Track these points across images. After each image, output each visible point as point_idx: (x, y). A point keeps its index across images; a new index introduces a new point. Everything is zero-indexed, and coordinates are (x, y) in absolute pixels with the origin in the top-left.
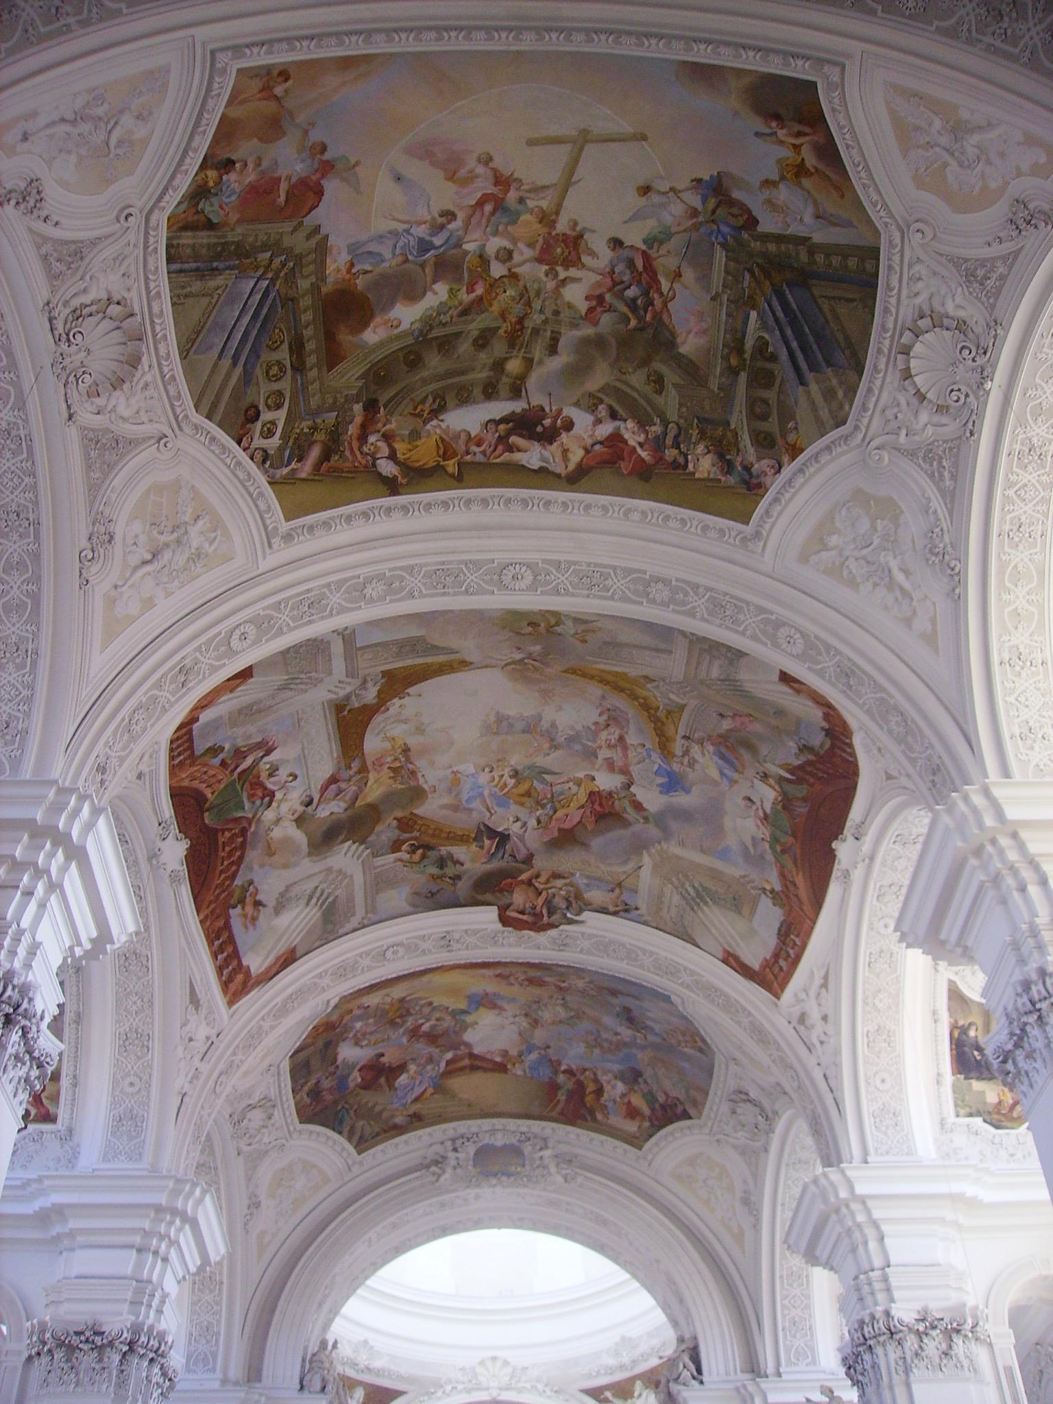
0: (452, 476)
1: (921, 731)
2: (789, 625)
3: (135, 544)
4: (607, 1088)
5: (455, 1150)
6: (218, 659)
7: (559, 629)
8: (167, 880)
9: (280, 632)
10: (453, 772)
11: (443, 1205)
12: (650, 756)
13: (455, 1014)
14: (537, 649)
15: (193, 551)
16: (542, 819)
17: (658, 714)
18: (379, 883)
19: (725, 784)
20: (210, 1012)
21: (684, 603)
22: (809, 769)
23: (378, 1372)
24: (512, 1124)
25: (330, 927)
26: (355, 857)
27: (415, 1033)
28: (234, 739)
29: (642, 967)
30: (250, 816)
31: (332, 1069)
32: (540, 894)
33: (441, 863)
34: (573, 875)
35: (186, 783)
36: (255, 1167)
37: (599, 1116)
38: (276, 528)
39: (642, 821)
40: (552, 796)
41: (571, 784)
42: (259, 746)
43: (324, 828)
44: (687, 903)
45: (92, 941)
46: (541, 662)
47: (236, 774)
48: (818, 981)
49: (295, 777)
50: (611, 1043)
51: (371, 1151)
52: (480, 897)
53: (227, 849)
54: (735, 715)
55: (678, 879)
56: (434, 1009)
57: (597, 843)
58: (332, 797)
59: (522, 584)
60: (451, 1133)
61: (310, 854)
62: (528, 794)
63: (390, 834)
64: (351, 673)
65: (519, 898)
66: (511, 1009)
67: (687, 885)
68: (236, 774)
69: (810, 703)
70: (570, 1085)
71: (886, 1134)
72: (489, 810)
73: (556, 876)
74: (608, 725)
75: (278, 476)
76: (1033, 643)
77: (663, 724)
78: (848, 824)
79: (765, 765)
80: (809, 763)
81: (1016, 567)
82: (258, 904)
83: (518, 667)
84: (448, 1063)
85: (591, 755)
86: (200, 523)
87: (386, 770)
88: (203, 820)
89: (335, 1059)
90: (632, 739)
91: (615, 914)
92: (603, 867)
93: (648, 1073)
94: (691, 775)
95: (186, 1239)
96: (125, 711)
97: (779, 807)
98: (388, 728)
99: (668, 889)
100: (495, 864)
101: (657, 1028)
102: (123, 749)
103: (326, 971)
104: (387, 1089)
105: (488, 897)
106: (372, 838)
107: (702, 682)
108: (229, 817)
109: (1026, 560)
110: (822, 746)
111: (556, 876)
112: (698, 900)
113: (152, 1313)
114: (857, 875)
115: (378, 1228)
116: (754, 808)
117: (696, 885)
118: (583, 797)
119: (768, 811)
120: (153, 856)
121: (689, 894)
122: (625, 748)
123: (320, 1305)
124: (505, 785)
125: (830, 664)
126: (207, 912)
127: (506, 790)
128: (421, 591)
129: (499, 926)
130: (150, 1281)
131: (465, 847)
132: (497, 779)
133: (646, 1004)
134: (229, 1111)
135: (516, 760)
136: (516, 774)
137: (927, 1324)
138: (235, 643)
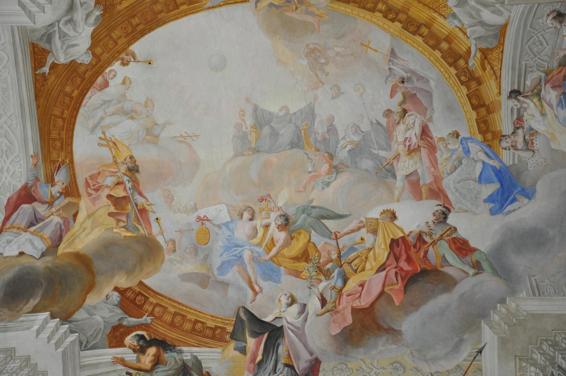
10: (199, 219)
12: (467, 152)
17: (471, 62)
26: (53, 341)
39: (471, 271)
40: (339, 257)
43: (9, 275)
55: (543, 354)
58: (23, 225)
62: (304, 256)
63: (107, 315)
74: (405, 111)
77: (479, 82)
87: (105, 201)
98: (107, 121)
106: (80, 315)
122: (432, 149)
124: (273, 242)
127: (274, 251)
131: (219, 350)
132: (261, 232)
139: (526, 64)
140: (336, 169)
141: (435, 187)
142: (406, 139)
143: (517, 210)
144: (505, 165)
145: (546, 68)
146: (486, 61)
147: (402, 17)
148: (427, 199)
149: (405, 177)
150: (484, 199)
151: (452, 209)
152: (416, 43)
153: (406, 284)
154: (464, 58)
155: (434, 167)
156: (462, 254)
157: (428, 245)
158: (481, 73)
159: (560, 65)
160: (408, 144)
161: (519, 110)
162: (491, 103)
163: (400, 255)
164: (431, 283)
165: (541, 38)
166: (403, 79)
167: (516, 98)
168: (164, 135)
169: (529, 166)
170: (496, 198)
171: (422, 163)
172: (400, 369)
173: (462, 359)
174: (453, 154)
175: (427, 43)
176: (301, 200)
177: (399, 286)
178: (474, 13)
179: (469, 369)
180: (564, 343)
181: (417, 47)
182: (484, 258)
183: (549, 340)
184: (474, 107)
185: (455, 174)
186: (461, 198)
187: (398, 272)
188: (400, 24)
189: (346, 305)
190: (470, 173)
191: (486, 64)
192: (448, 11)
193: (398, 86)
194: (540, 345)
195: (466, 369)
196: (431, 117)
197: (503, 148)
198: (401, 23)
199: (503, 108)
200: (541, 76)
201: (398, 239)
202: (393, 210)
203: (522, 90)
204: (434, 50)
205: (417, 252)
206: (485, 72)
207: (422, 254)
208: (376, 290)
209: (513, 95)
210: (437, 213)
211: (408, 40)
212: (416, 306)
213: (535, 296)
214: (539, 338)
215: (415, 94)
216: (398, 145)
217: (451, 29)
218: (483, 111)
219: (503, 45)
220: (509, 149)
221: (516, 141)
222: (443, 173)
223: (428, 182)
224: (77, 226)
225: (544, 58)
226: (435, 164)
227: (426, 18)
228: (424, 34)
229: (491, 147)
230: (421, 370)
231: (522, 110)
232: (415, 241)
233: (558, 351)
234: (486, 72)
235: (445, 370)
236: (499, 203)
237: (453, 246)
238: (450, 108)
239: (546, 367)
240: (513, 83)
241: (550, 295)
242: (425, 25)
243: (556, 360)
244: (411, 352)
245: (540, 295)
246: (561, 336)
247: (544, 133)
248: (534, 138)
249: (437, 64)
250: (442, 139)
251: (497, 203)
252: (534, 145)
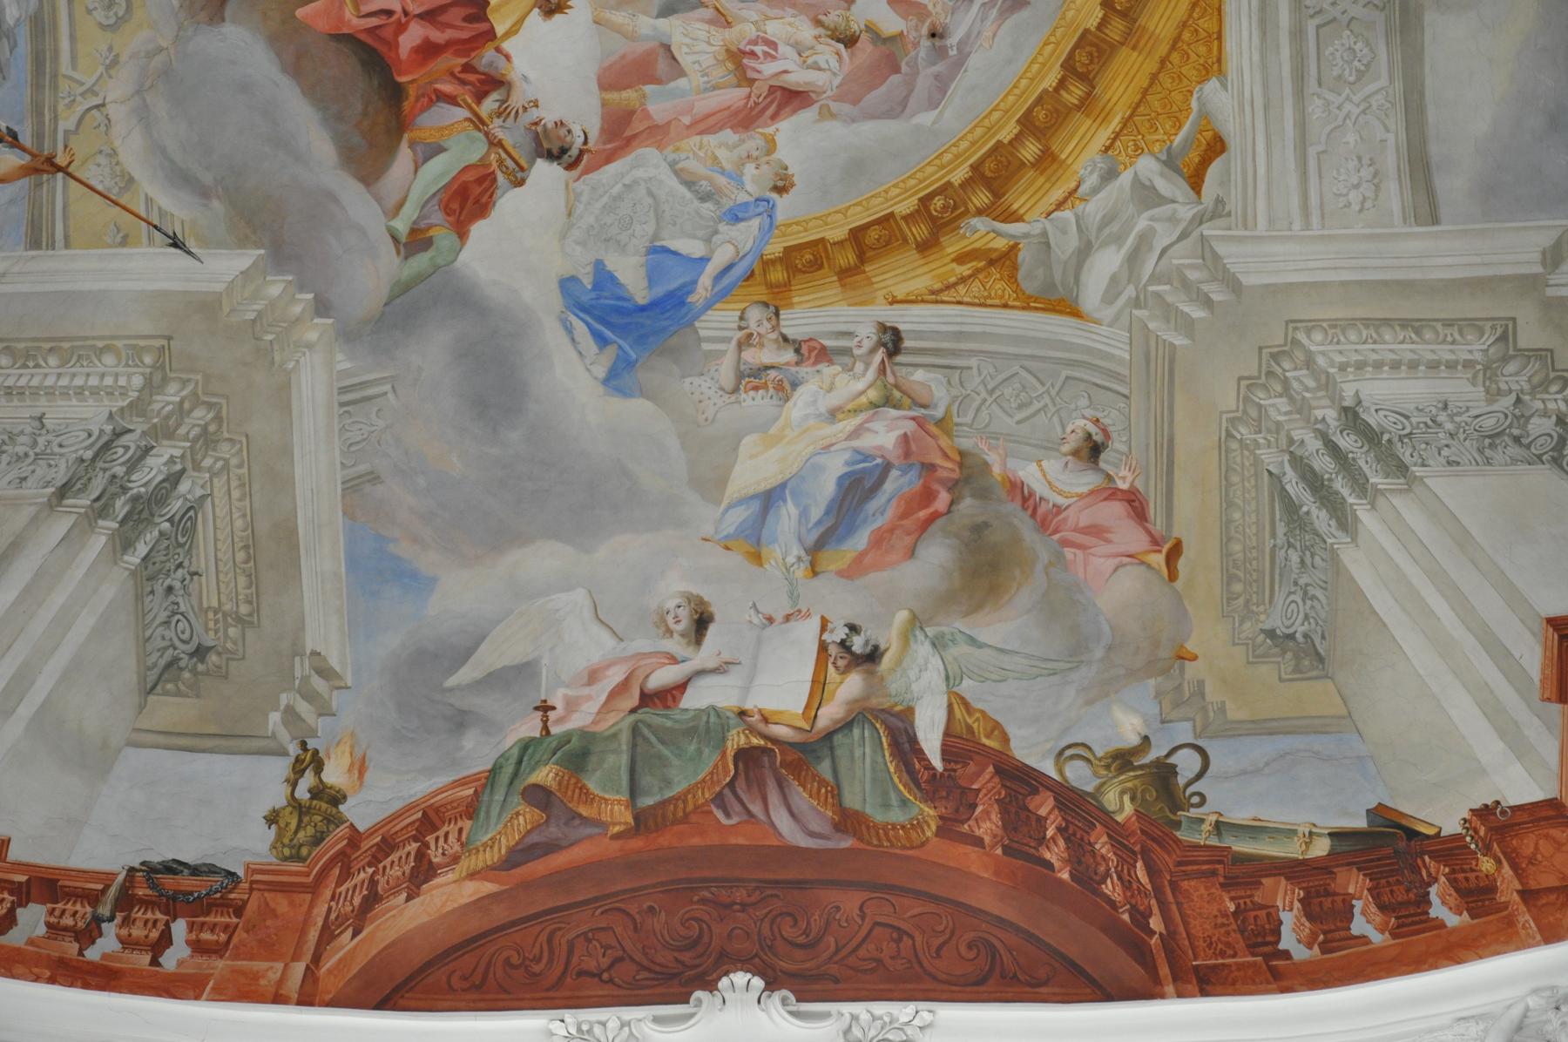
12: (735, 216)
17: (981, 224)
22: (1044, 806)
39: (402, 225)
44: (86, 467)
54: (1135, 504)
55: (181, 411)
74: (850, 41)
77: (924, 247)
78: (903, 1011)
79: (922, 649)
92: (117, 90)
97: (737, 739)
112: (121, 507)
116: (675, 646)
117: (184, 487)
119: (693, 700)
121: (133, 465)
122: (745, 119)
139: (970, 368)
141: (637, 126)
142: (772, 44)
143: (576, 348)
144: (697, 317)
145: (956, 420)
146: (982, 264)
147: (1117, 28)
148: (604, 104)
149: (665, 41)
150: (606, 263)
151: (575, 173)
152: (1039, 72)
153: (359, 40)
154: (993, 204)
155: (695, 123)
156: (449, 200)
157: (474, 105)
158: (949, 250)
159: (962, 454)
160: (759, 49)
161: (846, 352)
162: (869, 278)
163: (444, 26)
164: (365, 114)
165: (1037, 405)
166: (942, 37)
167: (881, 344)
169: (697, 381)
170: (605, 294)
171: (706, 90)
172: (111, 13)
173: (151, 194)
174: (730, 177)
175: (1039, 101)
177: (353, 21)
178: (1115, 227)
179: (123, 212)
180: (215, 463)
181: (1029, 75)
182: (440, 261)
183: (220, 427)
184: (857, 234)
185: (673, 182)
186: (605, 199)
187: (394, 18)
188: (1095, 24)
190: (675, 224)
191: (974, 264)
192: (1123, 158)
193: (923, 22)
194: (204, 403)
195: (122, 201)
196: (833, 116)
197: (743, 311)
198: (1100, 26)
199: (853, 311)
200: (935, 406)
201: (488, 20)
202: (570, 7)
203: (899, 359)
204: (1018, 121)
205: (452, 74)
206: (953, 261)
207: (447, 88)
209: (887, 338)
210: (563, 132)
211: (1049, 49)
212: (296, 67)
213: (339, 394)
214: (223, 401)
215: (897, 70)
216: (755, 23)
217: (1075, 167)
218: (848, 257)
219: (1024, 308)
220: (741, 328)
221: (762, 345)
222: (677, 149)
223: (652, 108)
225: (984, 414)
226: (702, 126)
227: (1107, 96)
228: (1063, 93)
229: (747, 279)
230: (110, 77)
231: (847, 360)
232: (482, 69)
233: (191, 447)
234: (954, 265)
235: (117, 143)
236: (593, 302)
237: (469, 177)
238: (856, 167)
239: (144, 415)
240: (919, 335)
241: (343, 429)
242: (1089, 94)
243: (165, 442)
244: (160, 50)
245: (342, 405)
246: (233, 455)
247: (783, 418)
248: (771, 391)
249: (979, 131)
250: (771, 145)
251: (593, 295)
252: (752, 393)
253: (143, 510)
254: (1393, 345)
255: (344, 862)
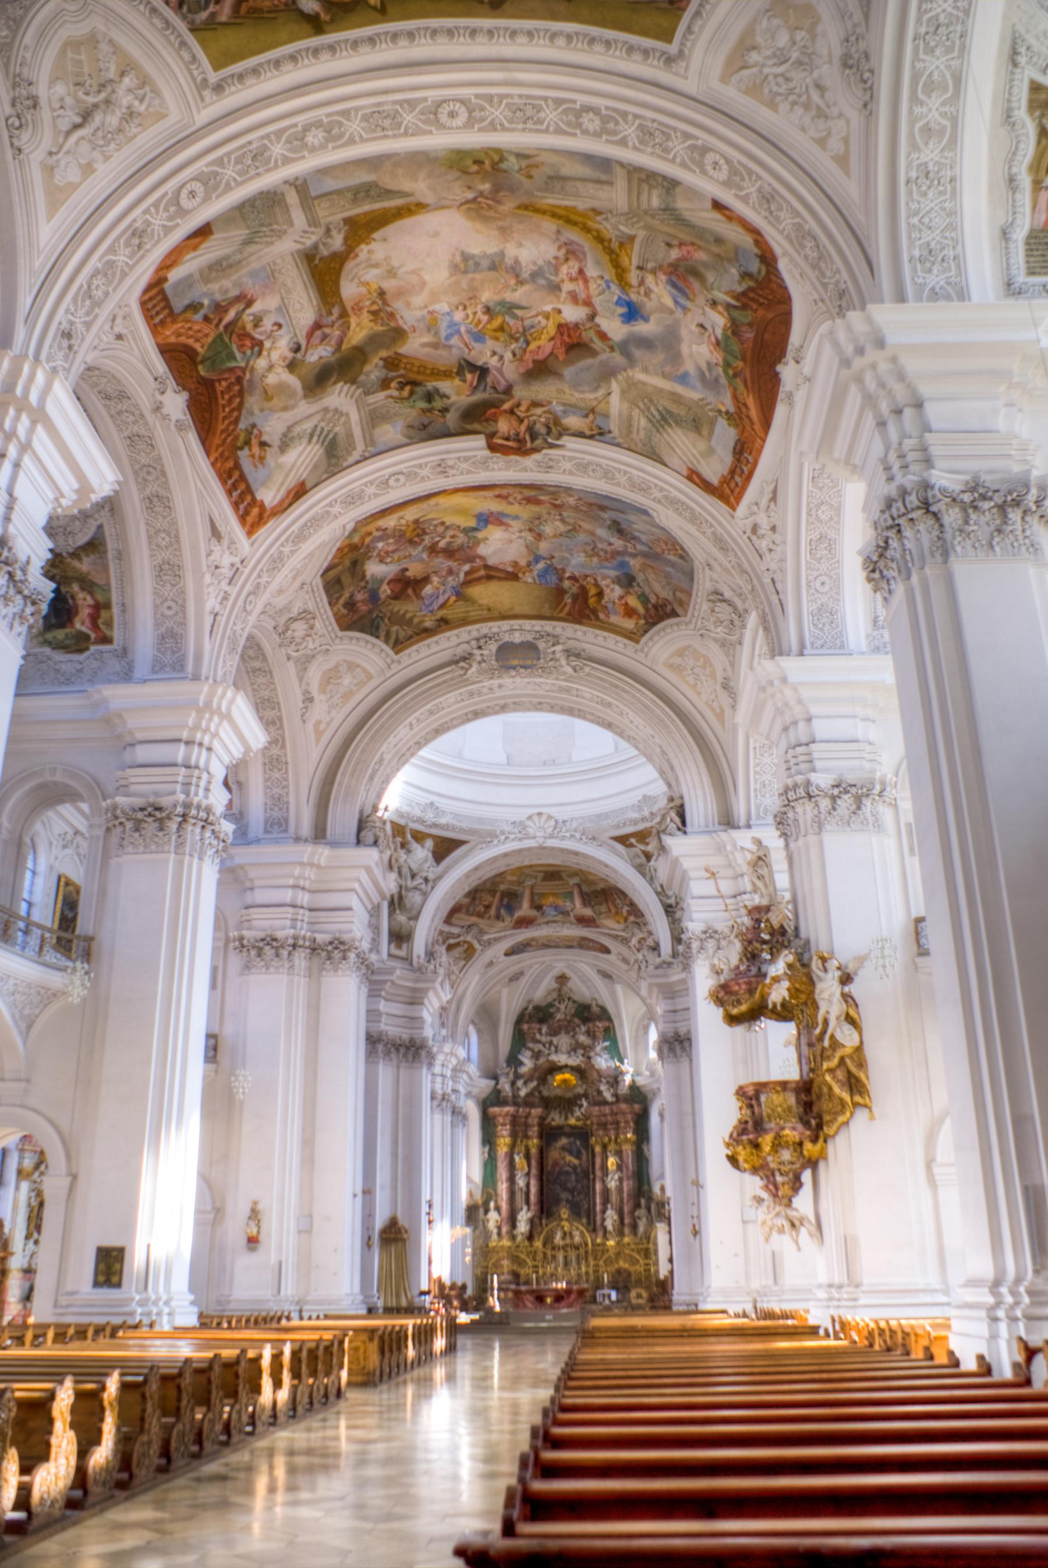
0: (374, 8)
1: (830, 255)
2: (713, 150)
3: (62, 107)
4: (607, 591)
5: (480, 648)
6: (171, 218)
7: (504, 166)
8: (173, 428)
9: (228, 188)
10: (431, 313)
11: (471, 694)
12: (609, 287)
13: (466, 531)
14: (486, 187)
15: (124, 110)
16: (517, 352)
18: (374, 419)
19: (679, 313)
20: (232, 542)
21: (615, 133)
22: (751, 295)
23: (445, 827)
24: (527, 624)
25: (333, 461)
27: (433, 550)
28: (212, 294)
29: (618, 484)
30: (243, 364)
31: (363, 584)
32: (521, 421)
33: (429, 397)
34: (550, 403)
35: (173, 339)
36: (305, 669)
37: (602, 616)
38: (205, 80)
41: (540, 318)
42: (238, 299)
43: (316, 371)
45: (77, 491)
46: (493, 200)
47: (221, 328)
48: (768, 496)
49: (280, 326)
50: (606, 552)
51: (408, 651)
52: (469, 427)
53: (227, 397)
54: (681, 244)
56: (447, 528)
57: (568, 372)
59: (460, 121)
60: (475, 634)
61: (305, 396)
62: (501, 329)
64: (313, 222)
65: (503, 426)
66: (516, 525)
67: (653, 409)
68: (221, 328)
69: (740, 230)
70: (575, 589)
71: (822, 630)
72: (466, 345)
73: (535, 404)
74: (567, 259)
75: (198, 21)
76: (943, 160)
77: (617, 255)
78: (790, 348)
80: (750, 289)
81: (930, 75)
82: (263, 444)
83: (472, 206)
84: (467, 574)
85: (555, 288)
86: (126, 80)
88: (197, 372)
89: (364, 576)
90: (591, 271)
91: (591, 437)
92: (577, 395)
93: (640, 577)
94: (649, 305)
95: (226, 732)
96: (82, 278)
97: (729, 333)
99: (636, 413)
100: (478, 396)
101: (644, 538)
102: (88, 314)
103: (336, 501)
104: (414, 598)
105: (476, 426)
106: (362, 378)
107: (646, 212)
108: (224, 367)
109: (942, 67)
110: (759, 272)
111: (535, 404)
113: (201, 792)
114: (800, 397)
115: (417, 714)
118: (552, 330)
119: (720, 337)
120: (158, 408)
122: (586, 281)
123: (371, 778)
124: (479, 321)
125: (753, 190)
126: (216, 455)
128: (361, 136)
129: (487, 453)
130: (197, 767)
133: (632, 517)
134: (273, 624)
135: (487, 296)
136: (488, 310)
137: (841, 787)
138: (185, 203)
140: (521, 282)
168: (400, 272)
176: (497, 298)
177: (563, 350)
189: (528, 357)
208: (548, 351)
224: (351, 333)
238: (598, 263)
253: (663, 418)
254: (644, 197)
255: (741, 418)
